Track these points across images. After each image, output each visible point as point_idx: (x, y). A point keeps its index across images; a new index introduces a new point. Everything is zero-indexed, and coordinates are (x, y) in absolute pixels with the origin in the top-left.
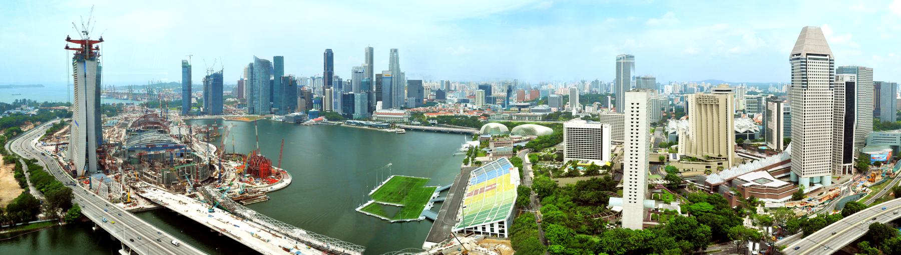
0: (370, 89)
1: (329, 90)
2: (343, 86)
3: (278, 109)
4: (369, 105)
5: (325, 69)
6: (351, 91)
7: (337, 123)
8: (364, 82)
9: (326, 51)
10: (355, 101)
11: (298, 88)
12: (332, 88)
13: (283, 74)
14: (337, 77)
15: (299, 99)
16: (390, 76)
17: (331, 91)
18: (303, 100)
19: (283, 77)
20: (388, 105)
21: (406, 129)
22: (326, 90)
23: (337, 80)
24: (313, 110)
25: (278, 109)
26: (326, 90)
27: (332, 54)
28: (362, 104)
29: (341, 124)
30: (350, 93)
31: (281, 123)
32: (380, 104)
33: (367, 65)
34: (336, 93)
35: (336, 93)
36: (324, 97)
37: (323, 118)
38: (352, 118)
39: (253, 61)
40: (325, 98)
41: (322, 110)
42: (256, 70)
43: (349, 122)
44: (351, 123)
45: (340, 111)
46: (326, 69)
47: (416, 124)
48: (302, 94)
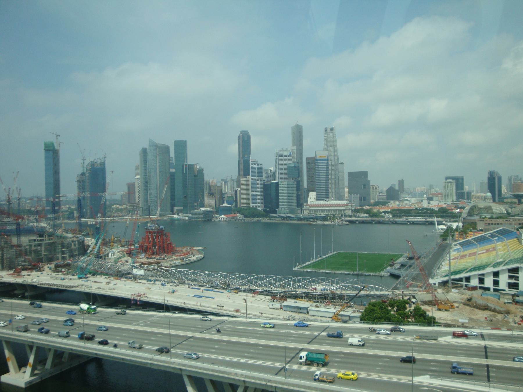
0: (299, 176)
1: (244, 179)
2: (264, 175)
3: (182, 208)
4: (298, 198)
5: (239, 158)
6: (274, 180)
7: (255, 219)
8: (292, 167)
9: (241, 133)
10: (280, 191)
11: (205, 182)
12: (249, 177)
13: (186, 162)
14: (255, 162)
15: (206, 195)
16: (326, 158)
17: (247, 182)
18: (212, 197)
19: (186, 165)
20: (323, 195)
21: (351, 222)
22: (242, 179)
23: (255, 166)
24: (225, 204)
25: (182, 208)
26: (242, 179)
27: (249, 137)
28: (289, 196)
29: (260, 220)
30: (273, 181)
31: (187, 221)
32: (312, 196)
33: (295, 148)
34: (254, 183)
35: (254, 183)
36: (239, 189)
37: (239, 216)
38: (276, 213)
39: (146, 146)
40: (240, 191)
41: (236, 206)
42: (150, 157)
43: (272, 217)
44: (275, 217)
45: (259, 206)
46: (241, 156)
47: (363, 217)
48: (210, 190)
